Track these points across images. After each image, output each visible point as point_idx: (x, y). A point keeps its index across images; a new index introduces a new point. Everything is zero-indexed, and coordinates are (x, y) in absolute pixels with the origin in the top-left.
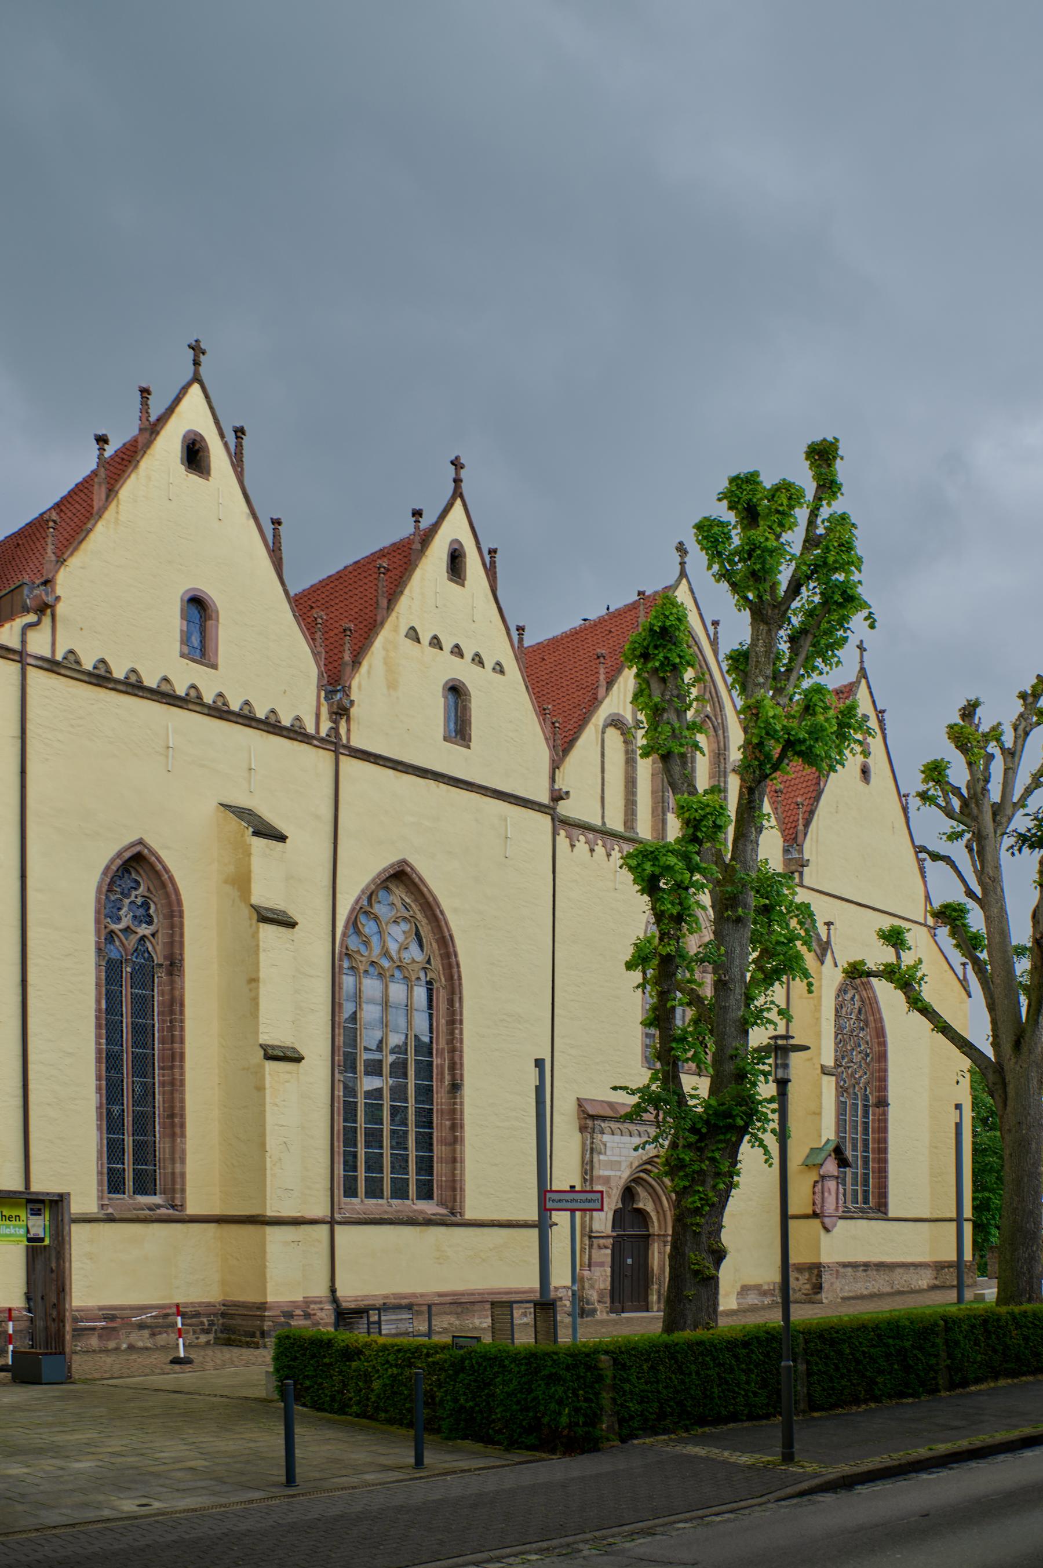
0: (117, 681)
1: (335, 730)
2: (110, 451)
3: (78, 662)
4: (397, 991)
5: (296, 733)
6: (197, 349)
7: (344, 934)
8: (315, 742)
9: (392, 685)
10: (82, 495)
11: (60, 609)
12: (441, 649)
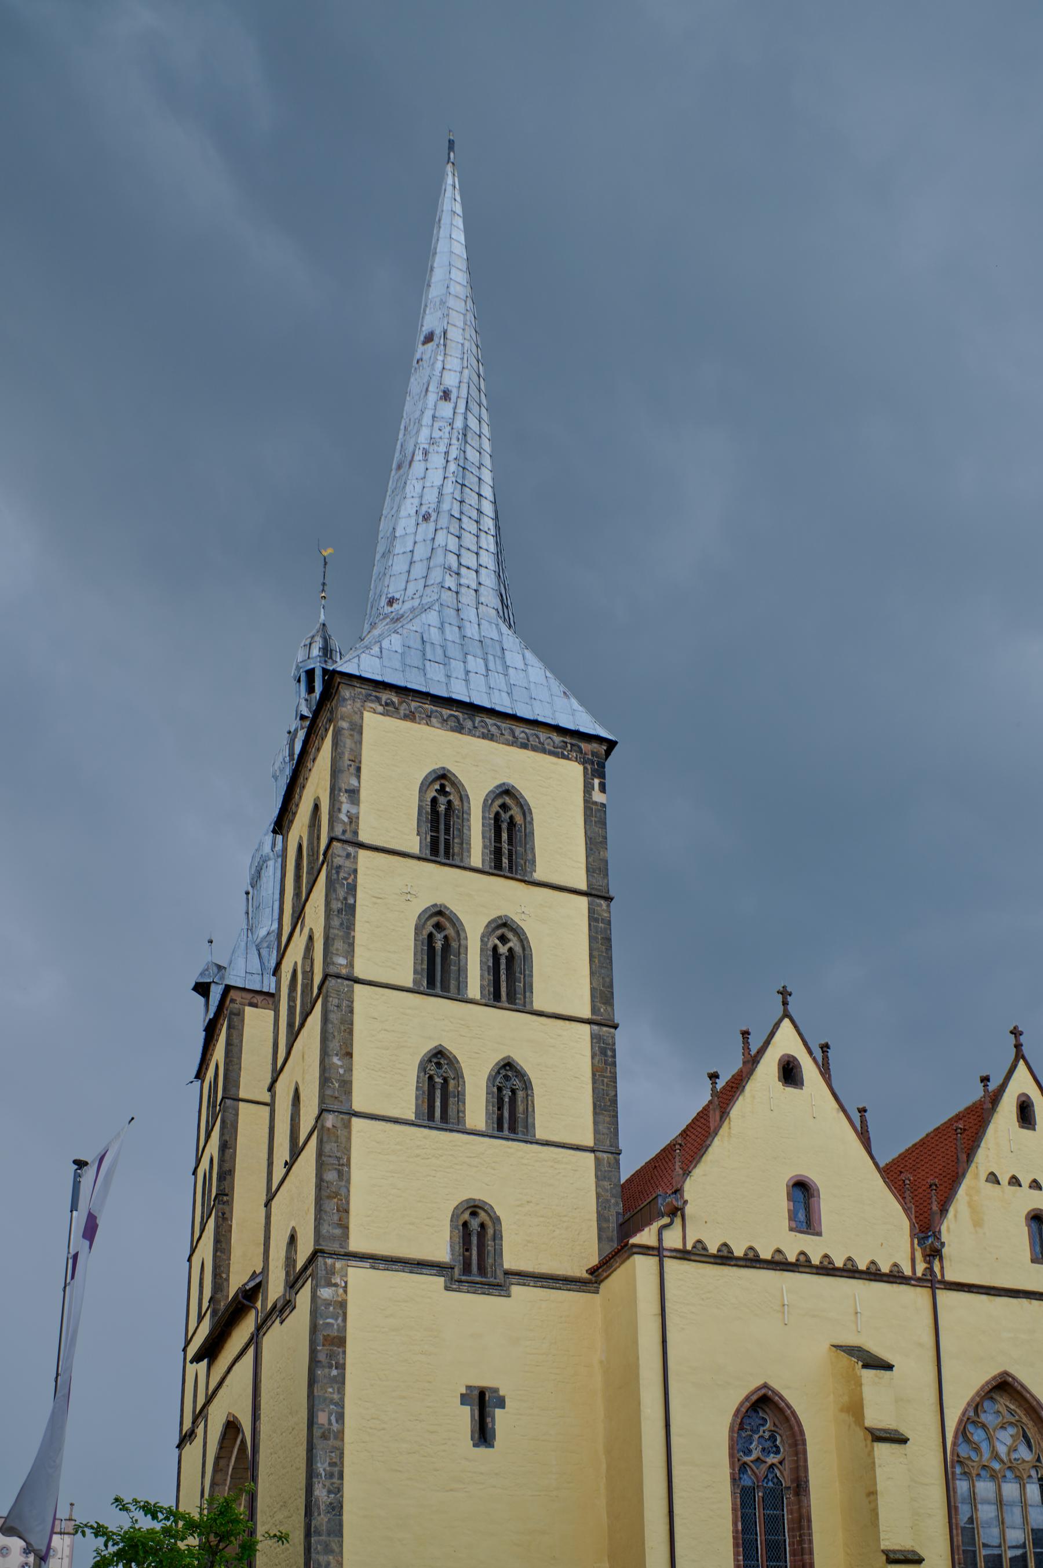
0: (738, 1259)
1: (930, 1269)
2: (721, 1084)
3: (705, 1249)
4: (1010, 1490)
5: (895, 1277)
7: (954, 1444)
8: (913, 1282)
9: (978, 1223)
10: (702, 1120)
11: (688, 1210)
12: (1020, 1186)
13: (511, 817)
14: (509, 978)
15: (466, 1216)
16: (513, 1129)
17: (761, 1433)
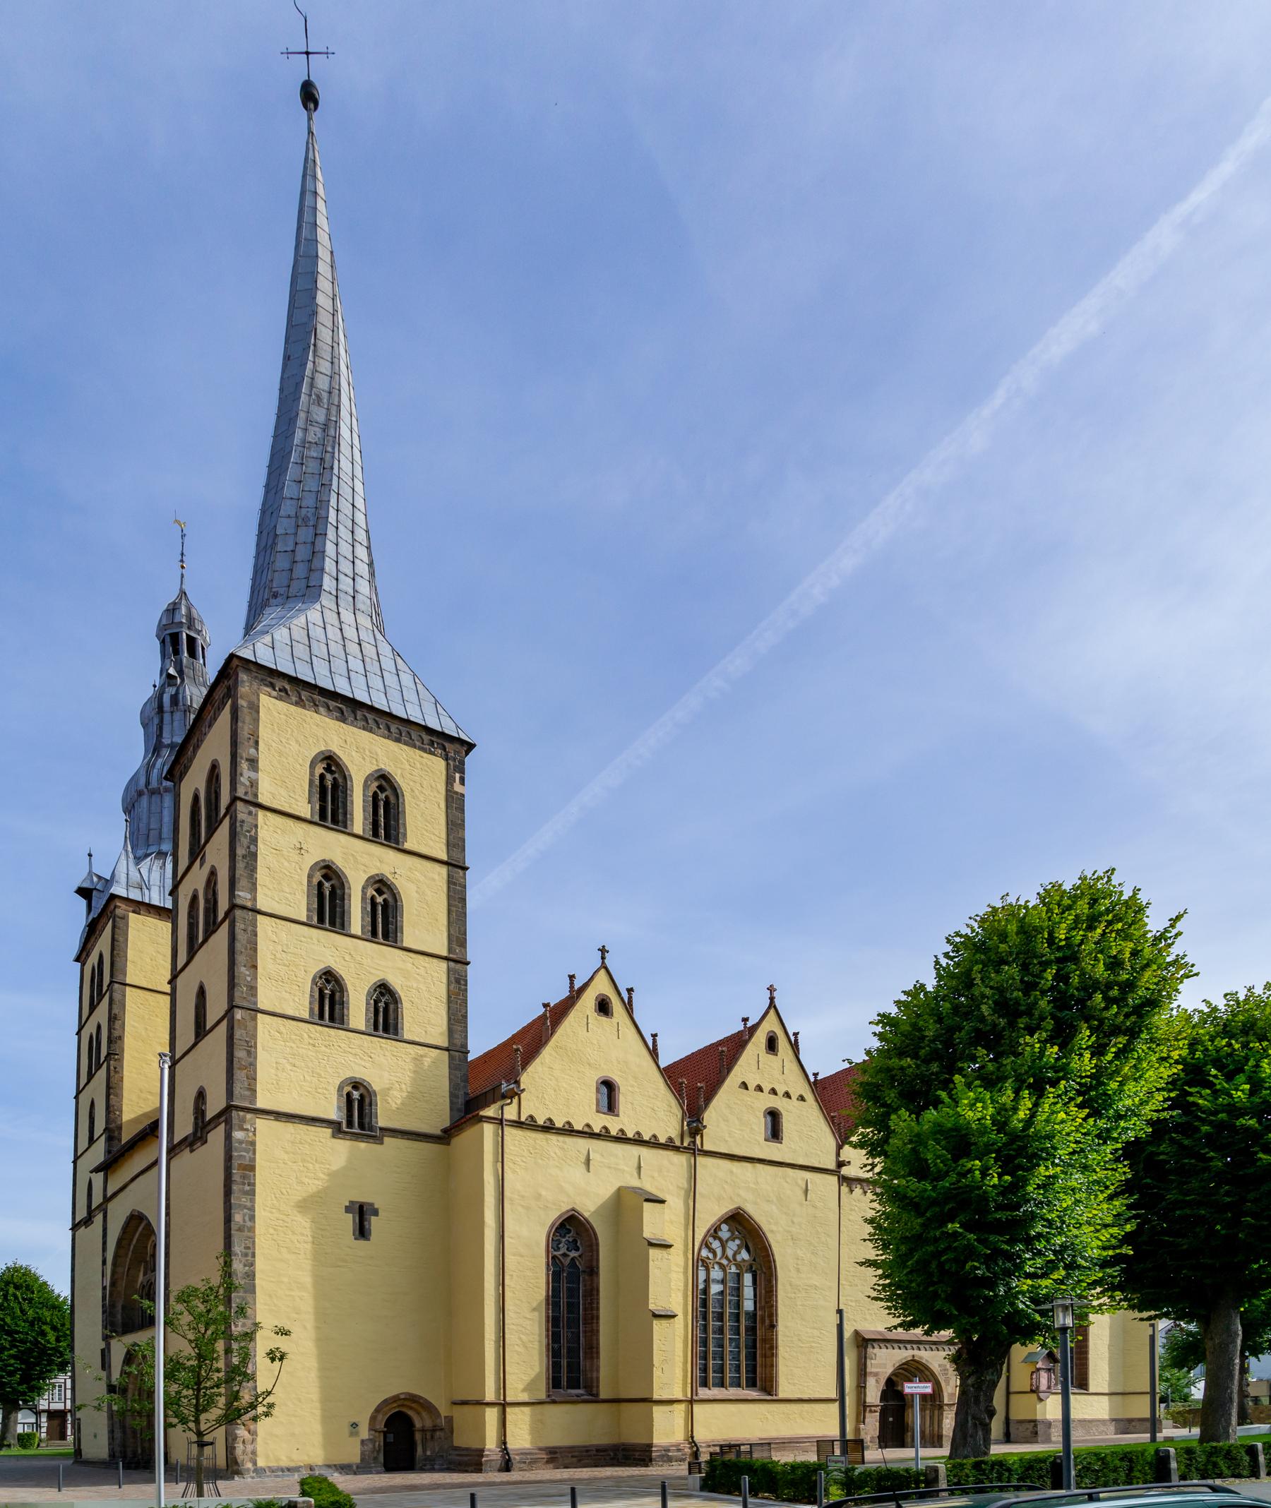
14: (385, 921)
15: (349, 1089)
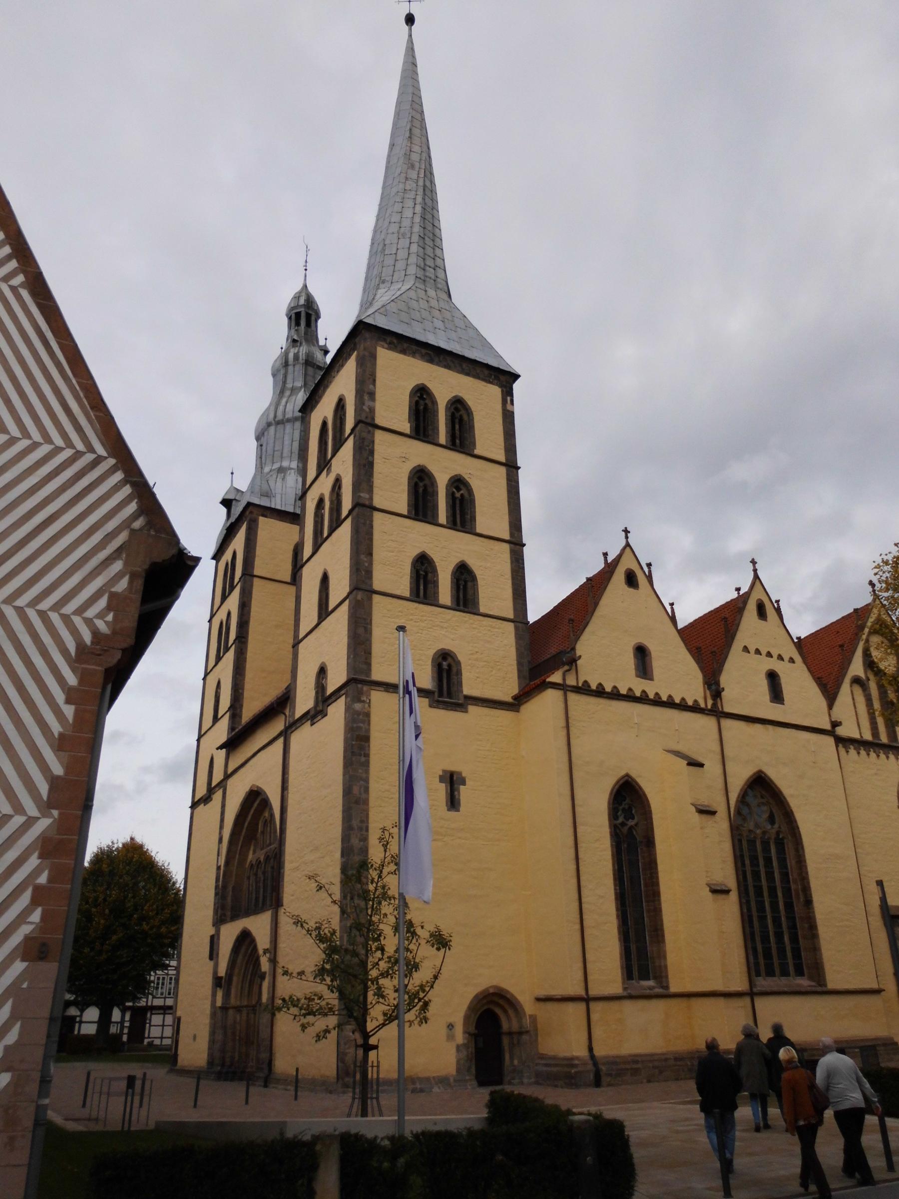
6: (626, 531)
13: (461, 416)
15: (440, 660)
16: (465, 605)
17: (623, 806)
